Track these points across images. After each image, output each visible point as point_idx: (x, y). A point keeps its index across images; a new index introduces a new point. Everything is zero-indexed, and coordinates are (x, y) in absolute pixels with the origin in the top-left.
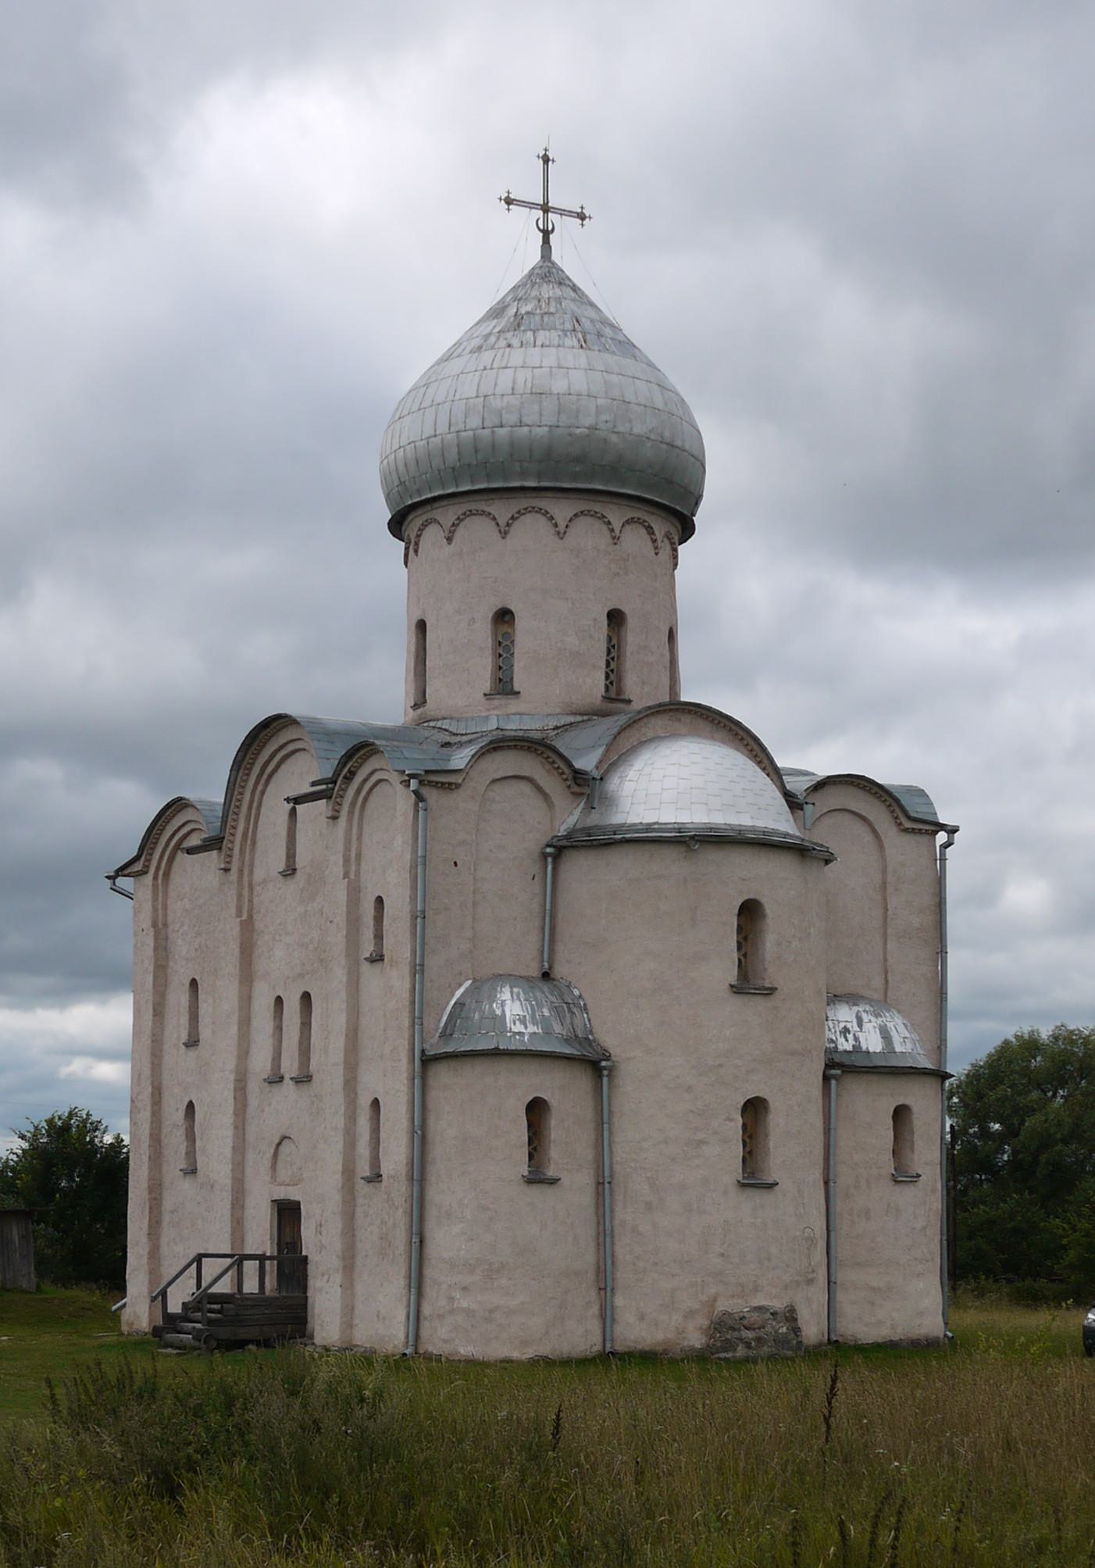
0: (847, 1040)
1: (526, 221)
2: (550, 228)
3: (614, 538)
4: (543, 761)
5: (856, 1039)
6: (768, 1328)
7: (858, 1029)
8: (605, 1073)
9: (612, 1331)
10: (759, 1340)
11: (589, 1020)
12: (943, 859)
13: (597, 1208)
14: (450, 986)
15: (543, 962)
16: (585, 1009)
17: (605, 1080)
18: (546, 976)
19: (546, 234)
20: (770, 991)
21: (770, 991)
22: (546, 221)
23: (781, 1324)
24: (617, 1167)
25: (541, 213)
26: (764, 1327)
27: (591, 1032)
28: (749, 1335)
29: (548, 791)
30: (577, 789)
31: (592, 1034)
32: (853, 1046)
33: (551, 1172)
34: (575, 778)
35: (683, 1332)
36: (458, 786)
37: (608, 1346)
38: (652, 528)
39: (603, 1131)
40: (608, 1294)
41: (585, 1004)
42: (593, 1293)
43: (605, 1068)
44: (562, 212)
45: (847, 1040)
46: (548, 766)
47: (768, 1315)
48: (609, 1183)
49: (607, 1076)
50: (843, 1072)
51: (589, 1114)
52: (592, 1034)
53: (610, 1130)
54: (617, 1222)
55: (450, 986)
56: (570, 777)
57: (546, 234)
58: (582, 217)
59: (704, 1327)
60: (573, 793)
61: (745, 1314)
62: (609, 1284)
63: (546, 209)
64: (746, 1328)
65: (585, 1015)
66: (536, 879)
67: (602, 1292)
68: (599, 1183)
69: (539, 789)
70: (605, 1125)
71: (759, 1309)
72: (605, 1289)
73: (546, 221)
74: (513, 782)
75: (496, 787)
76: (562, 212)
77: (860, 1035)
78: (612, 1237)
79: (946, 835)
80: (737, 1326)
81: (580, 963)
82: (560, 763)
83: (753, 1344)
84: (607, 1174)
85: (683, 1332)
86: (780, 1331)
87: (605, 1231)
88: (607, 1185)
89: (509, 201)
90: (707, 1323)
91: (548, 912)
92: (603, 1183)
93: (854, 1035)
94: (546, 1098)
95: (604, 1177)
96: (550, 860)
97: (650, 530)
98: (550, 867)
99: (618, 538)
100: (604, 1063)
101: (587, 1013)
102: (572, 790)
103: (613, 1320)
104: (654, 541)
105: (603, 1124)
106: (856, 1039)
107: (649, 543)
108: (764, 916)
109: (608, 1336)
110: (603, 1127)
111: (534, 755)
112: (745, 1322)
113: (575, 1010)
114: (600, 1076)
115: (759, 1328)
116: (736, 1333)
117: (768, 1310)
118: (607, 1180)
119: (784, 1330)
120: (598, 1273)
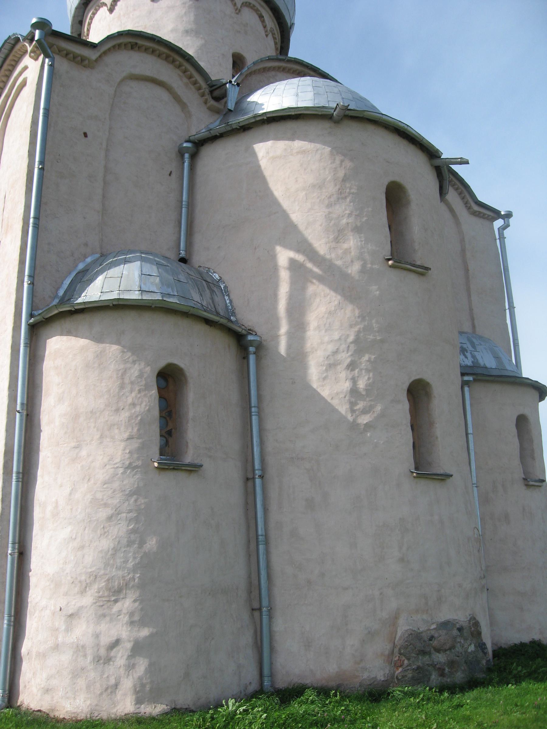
0: (466, 357)
3: (236, 10)
4: (181, 74)
5: (473, 357)
6: (458, 648)
7: (473, 350)
8: (252, 349)
9: (271, 664)
10: (452, 664)
11: (231, 301)
12: (502, 238)
13: (246, 510)
14: (72, 255)
15: (180, 250)
16: (226, 292)
17: (252, 358)
18: (183, 260)
23: (469, 642)
24: (271, 460)
26: (452, 647)
27: (234, 314)
28: (441, 658)
29: (185, 100)
30: (212, 102)
31: (235, 316)
32: (473, 362)
33: (189, 458)
34: (211, 92)
35: (361, 660)
37: (266, 683)
38: (263, 17)
39: (251, 416)
40: (265, 618)
41: (226, 287)
42: (246, 616)
43: (251, 343)
45: (466, 357)
46: (185, 80)
47: (455, 632)
48: (261, 477)
49: (254, 353)
50: (475, 380)
51: (234, 396)
52: (235, 316)
53: (259, 414)
54: (272, 525)
55: (72, 255)
56: (207, 91)
59: (387, 653)
60: (211, 109)
61: (433, 632)
62: (265, 602)
64: (438, 651)
65: (226, 298)
66: (173, 175)
67: (257, 614)
68: (248, 479)
69: (177, 99)
70: (253, 409)
71: (445, 625)
72: (260, 609)
74: (150, 85)
75: (134, 84)
77: (476, 353)
78: (267, 543)
79: (502, 221)
80: (427, 650)
81: (219, 247)
82: (197, 77)
83: (447, 670)
84: (257, 466)
85: (361, 660)
86: (469, 650)
87: (257, 536)
88: (258, 481)
90: (388, 647)
91: (184, 203)
92: (254, 478)
93: (471, 353)
94: (182, 365)
95: (254, 470)
96: (187, 156)
98: (186, 164)
99: (240, 11)
100: (250, 338)
101: (228, 295)
102: (208, 105)
103: (272, 649)
105: (250, 407)
106: (473, 357)
107: (262, 28)
108: (408, 203)
109: (266, 671)
110: (251, 412)
111: (171, 66)
112: (435, 643)
113: (215, 289)
114: (245, 357)
115: (450, 649)
116: (427, 657)
117: (454, 625)
118: (258, 473)
119: (472, 648)
120: (250, 592)
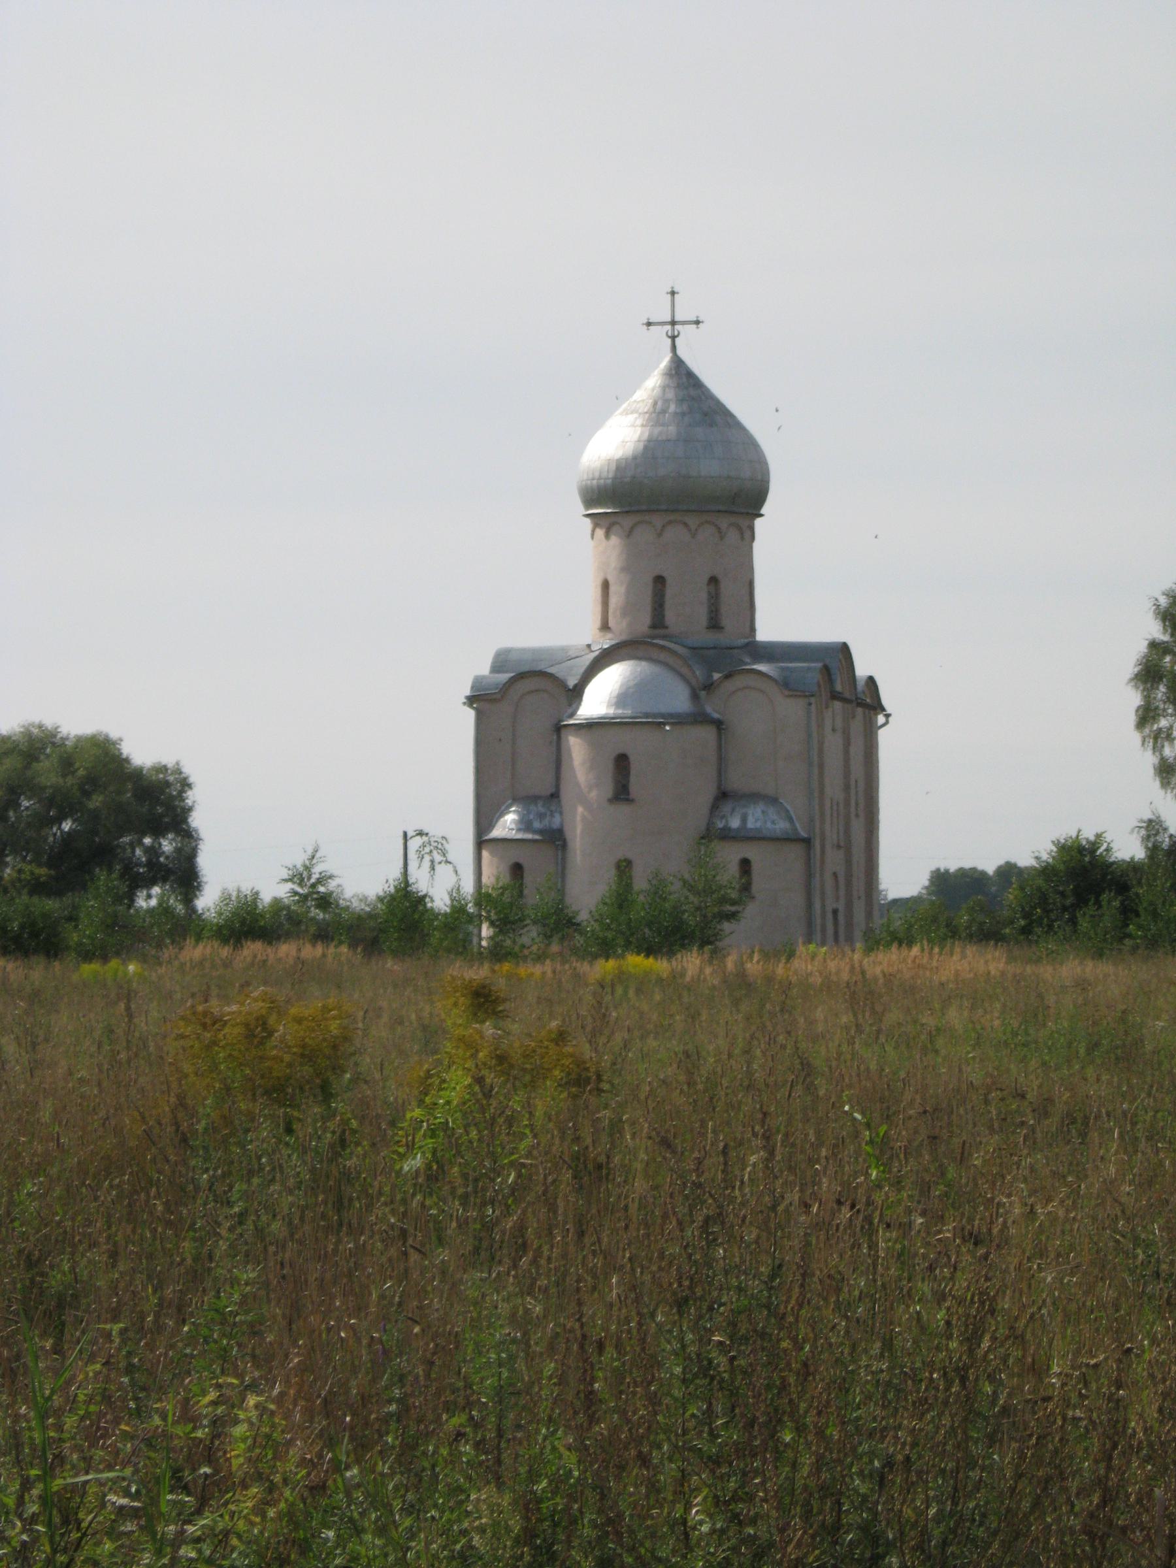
1: (661, 332)
2: (676, 333)
19: (673, 338)
20: (632, 801)
21: (632, 801)
22: (673, 330)
25: (669, 327)
36: (500, 700)
44: (684, 323)
57: (673, 338)
58: (697, 322)
63: (673, 323)
73: (673, 330)
76: (684, 323)
89: (649, 324)
97: (686, 525)
104: (690, 530)
106: (727, 821)
